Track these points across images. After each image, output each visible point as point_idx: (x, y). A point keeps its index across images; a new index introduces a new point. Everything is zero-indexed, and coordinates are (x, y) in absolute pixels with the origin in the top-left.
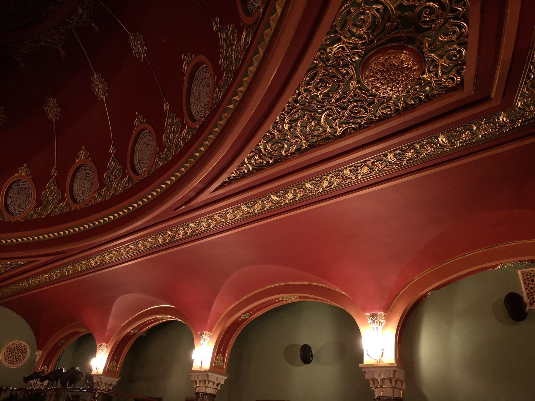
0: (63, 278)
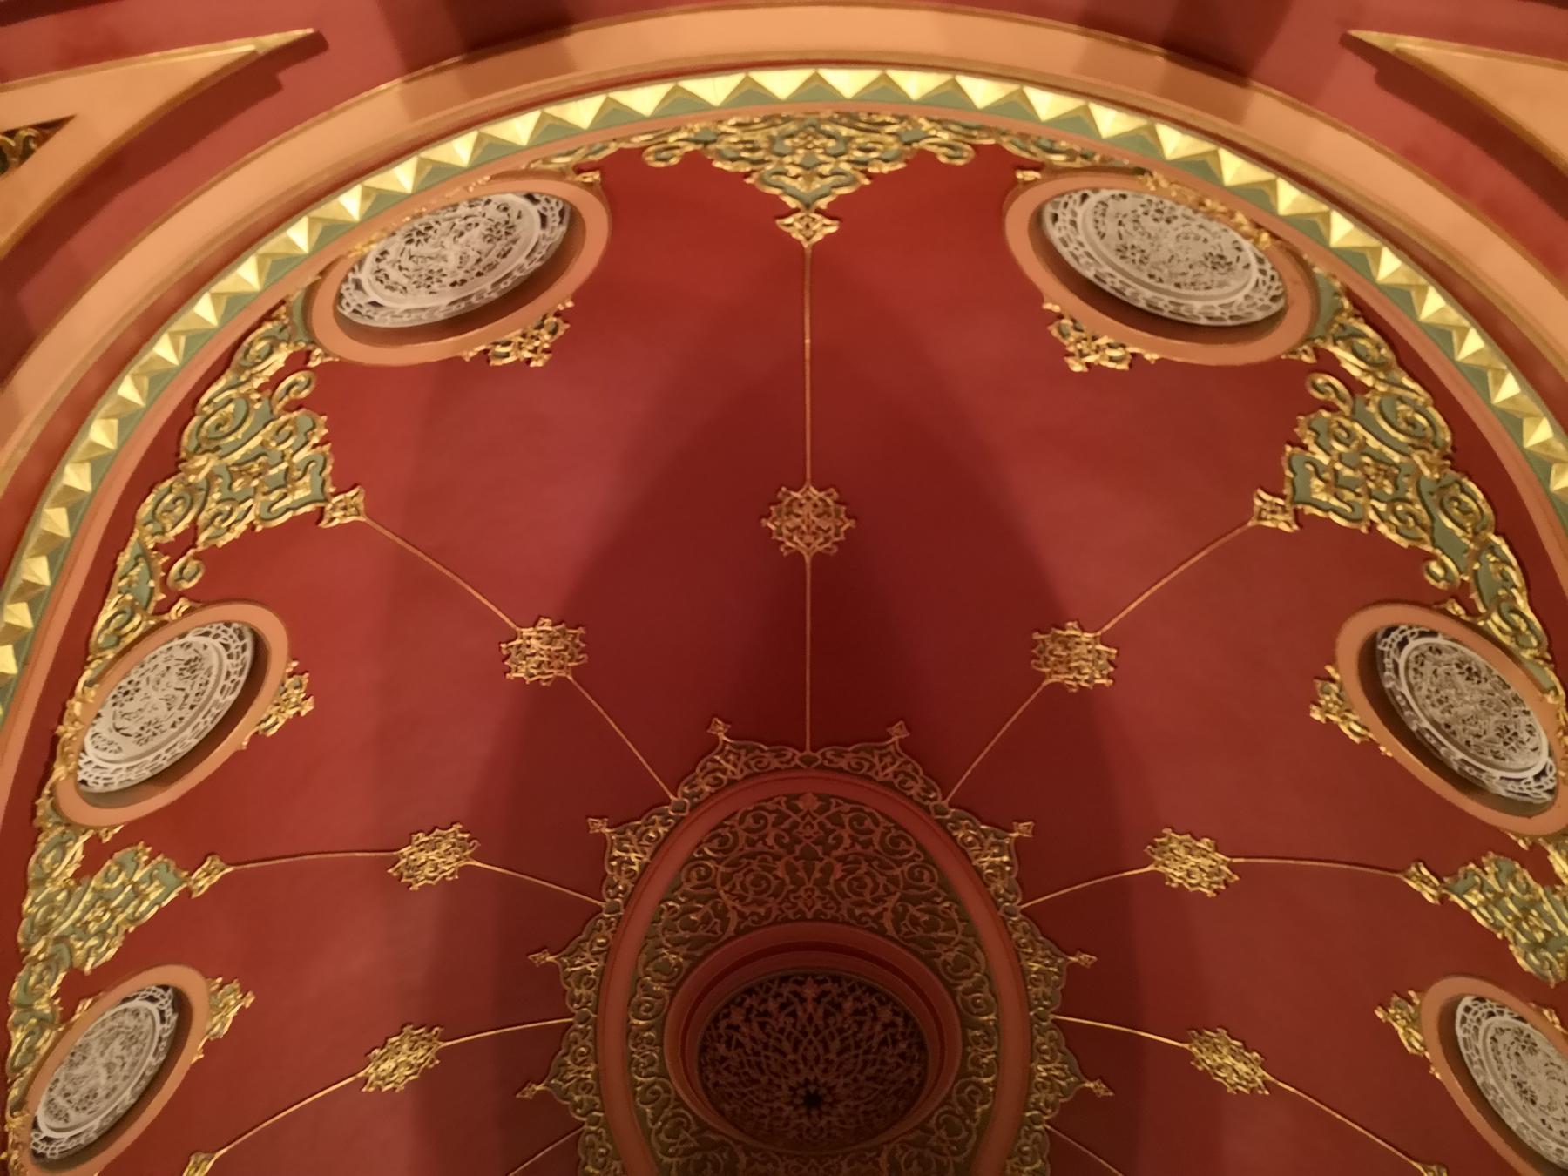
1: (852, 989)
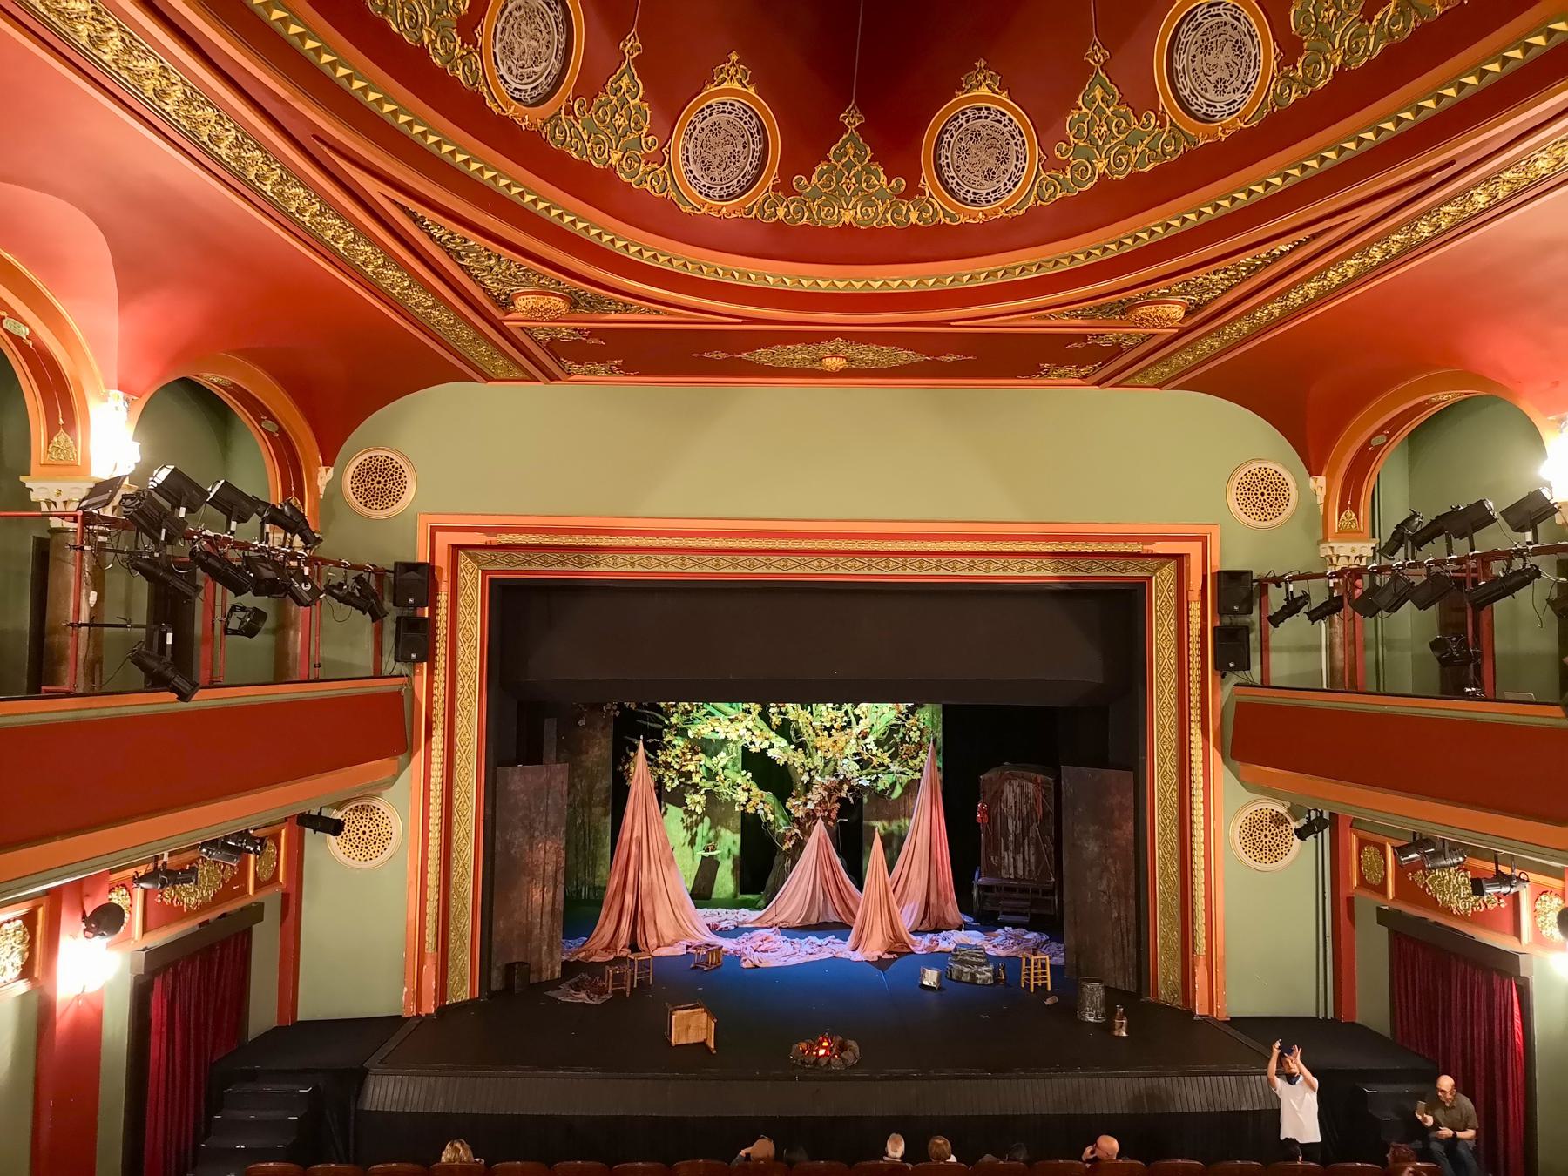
0: (1411, 251)
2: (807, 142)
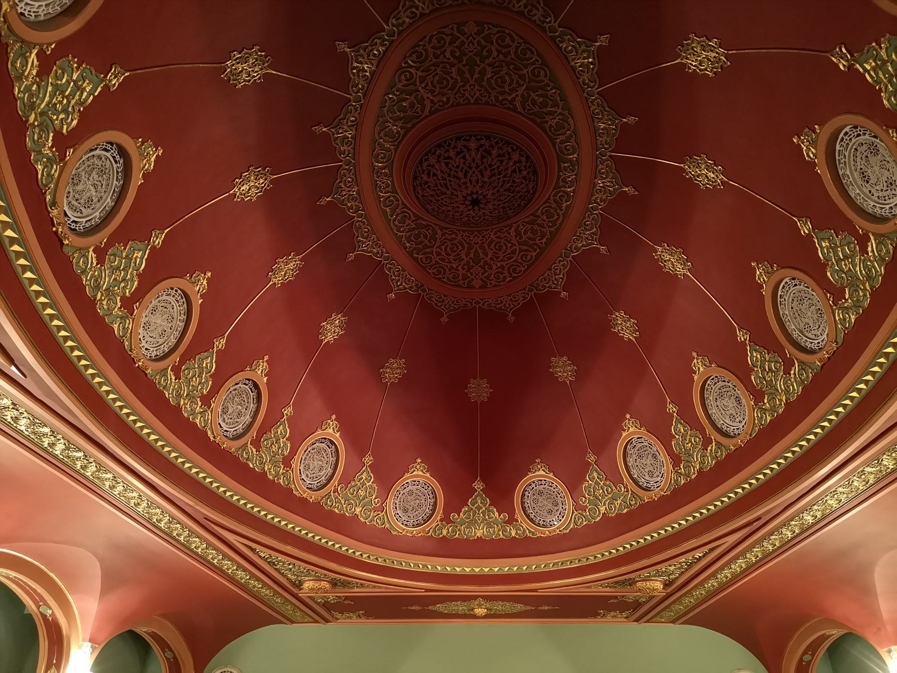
0: (767, 557)
1: (497, 143)
2: (457, 498)
